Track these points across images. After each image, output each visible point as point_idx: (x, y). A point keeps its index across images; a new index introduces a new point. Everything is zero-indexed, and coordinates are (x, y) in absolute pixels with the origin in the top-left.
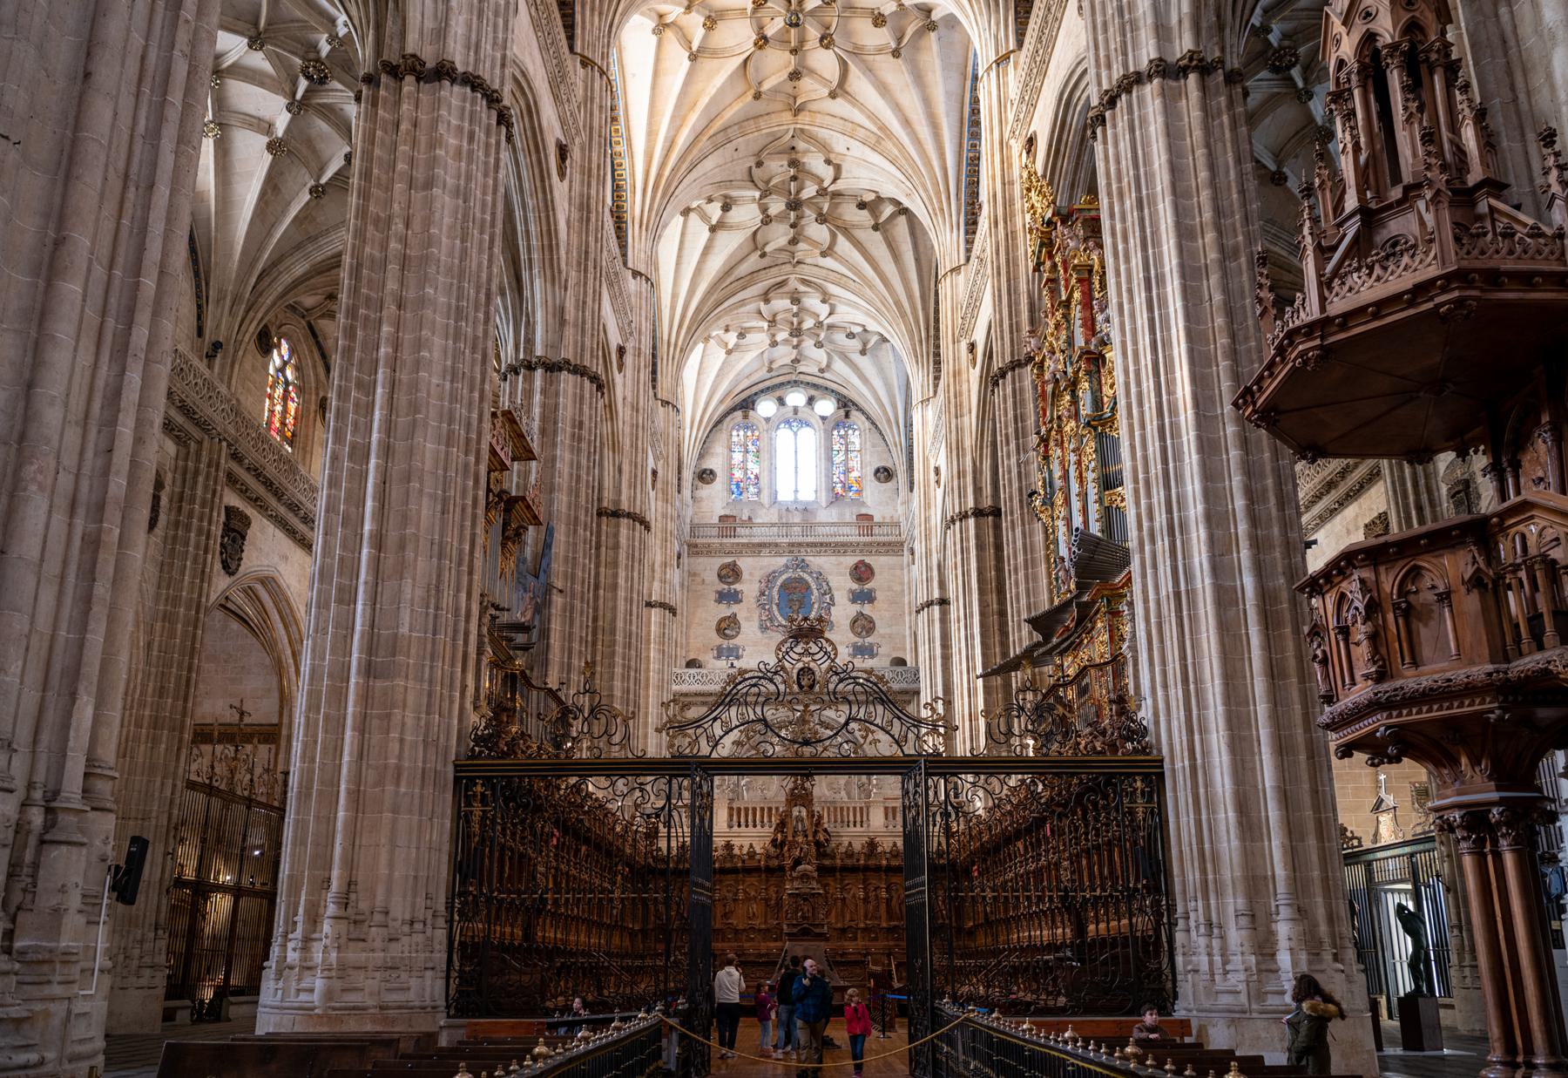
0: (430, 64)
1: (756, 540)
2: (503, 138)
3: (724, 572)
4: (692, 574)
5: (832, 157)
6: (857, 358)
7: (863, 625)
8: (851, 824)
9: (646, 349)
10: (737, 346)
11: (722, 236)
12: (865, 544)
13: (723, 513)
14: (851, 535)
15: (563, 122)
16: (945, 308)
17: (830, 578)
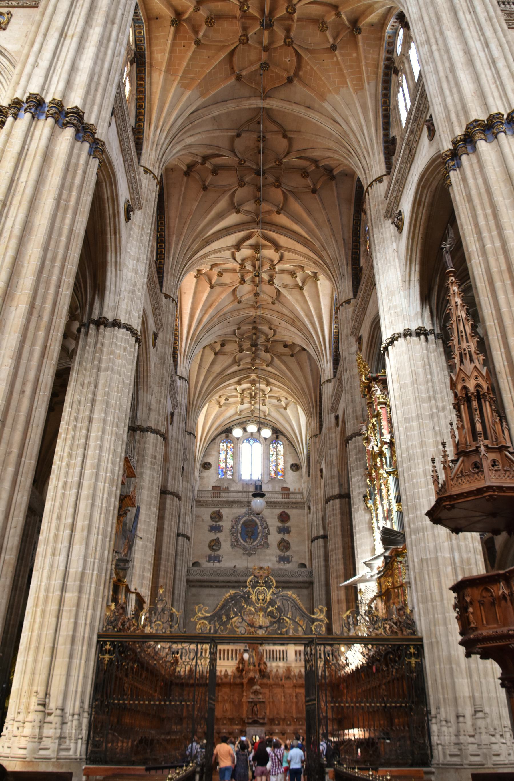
0: (111, 320)
1: (231, 499)
2: (137, 347)
3: (214, 516)
4: (197, 516)
5: (272, 326)
6: (282, 410)
7: (284, 545)
8: (278, 659)
9: (184, 412)
10: (225, 404)
11: (221, 358)
12: (286, 503)
13: (214, 485)
14: (278, 498)
15: (156, 323)
16: (324, 397)
17: (268, 520)
